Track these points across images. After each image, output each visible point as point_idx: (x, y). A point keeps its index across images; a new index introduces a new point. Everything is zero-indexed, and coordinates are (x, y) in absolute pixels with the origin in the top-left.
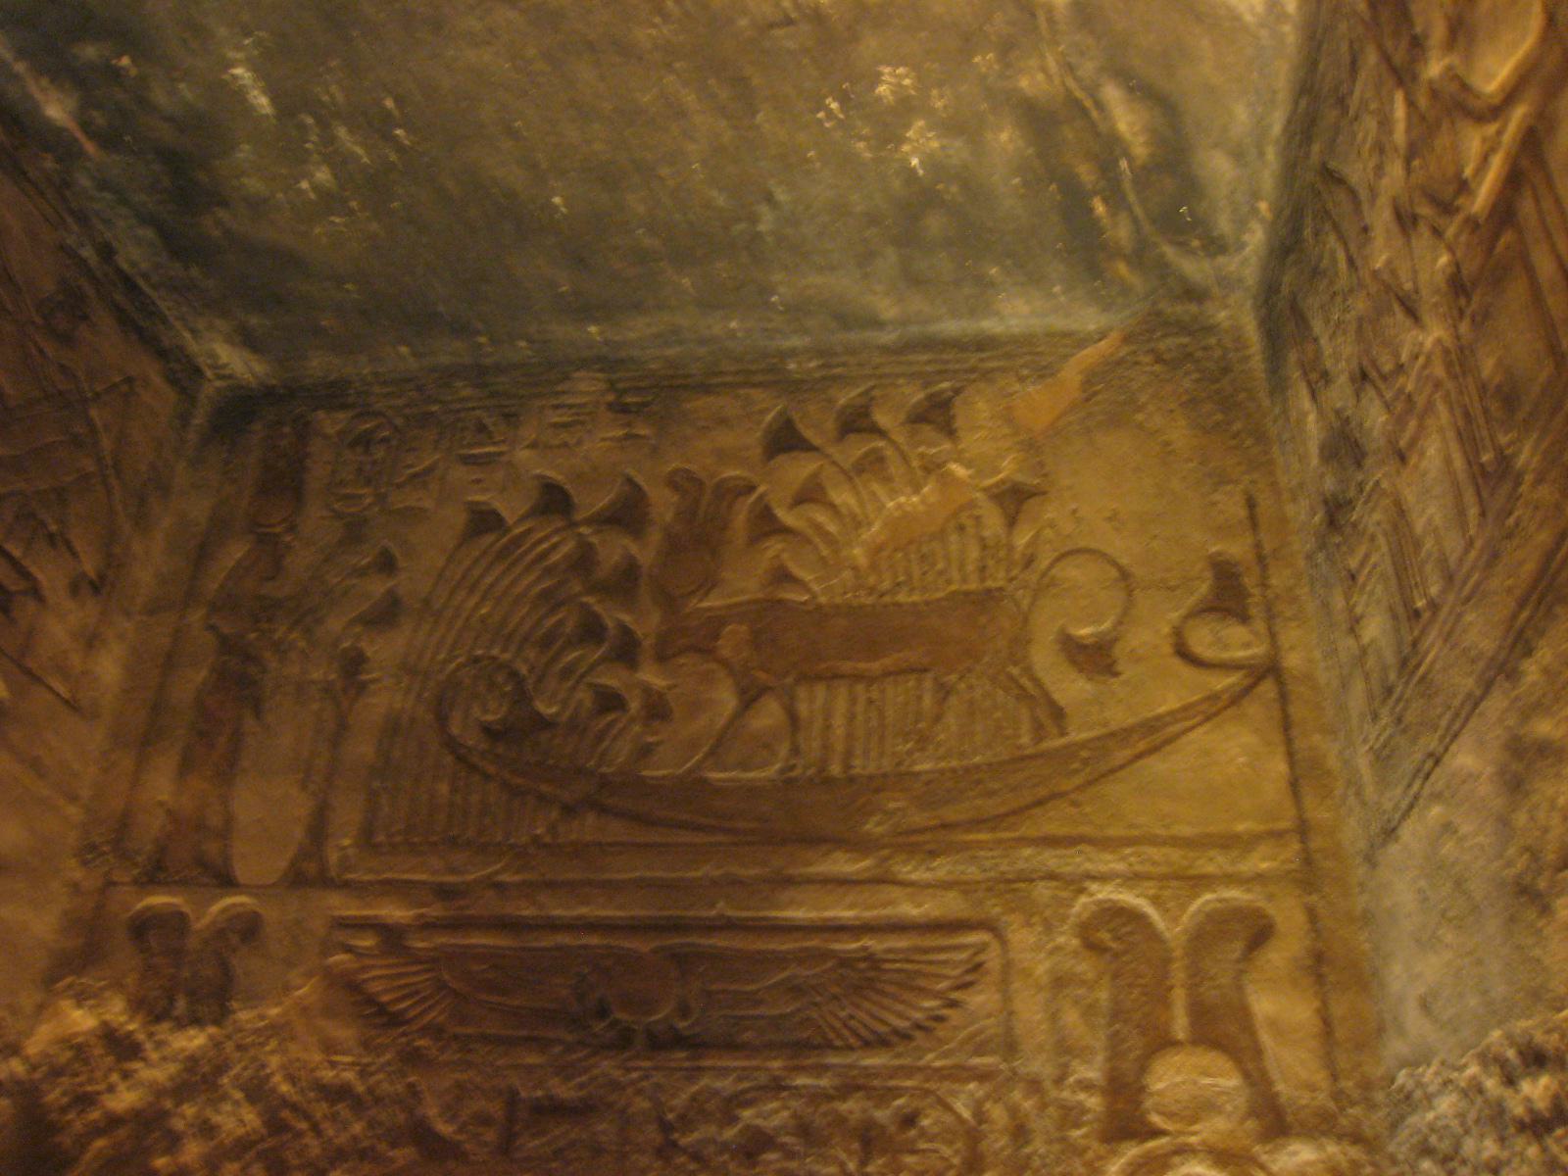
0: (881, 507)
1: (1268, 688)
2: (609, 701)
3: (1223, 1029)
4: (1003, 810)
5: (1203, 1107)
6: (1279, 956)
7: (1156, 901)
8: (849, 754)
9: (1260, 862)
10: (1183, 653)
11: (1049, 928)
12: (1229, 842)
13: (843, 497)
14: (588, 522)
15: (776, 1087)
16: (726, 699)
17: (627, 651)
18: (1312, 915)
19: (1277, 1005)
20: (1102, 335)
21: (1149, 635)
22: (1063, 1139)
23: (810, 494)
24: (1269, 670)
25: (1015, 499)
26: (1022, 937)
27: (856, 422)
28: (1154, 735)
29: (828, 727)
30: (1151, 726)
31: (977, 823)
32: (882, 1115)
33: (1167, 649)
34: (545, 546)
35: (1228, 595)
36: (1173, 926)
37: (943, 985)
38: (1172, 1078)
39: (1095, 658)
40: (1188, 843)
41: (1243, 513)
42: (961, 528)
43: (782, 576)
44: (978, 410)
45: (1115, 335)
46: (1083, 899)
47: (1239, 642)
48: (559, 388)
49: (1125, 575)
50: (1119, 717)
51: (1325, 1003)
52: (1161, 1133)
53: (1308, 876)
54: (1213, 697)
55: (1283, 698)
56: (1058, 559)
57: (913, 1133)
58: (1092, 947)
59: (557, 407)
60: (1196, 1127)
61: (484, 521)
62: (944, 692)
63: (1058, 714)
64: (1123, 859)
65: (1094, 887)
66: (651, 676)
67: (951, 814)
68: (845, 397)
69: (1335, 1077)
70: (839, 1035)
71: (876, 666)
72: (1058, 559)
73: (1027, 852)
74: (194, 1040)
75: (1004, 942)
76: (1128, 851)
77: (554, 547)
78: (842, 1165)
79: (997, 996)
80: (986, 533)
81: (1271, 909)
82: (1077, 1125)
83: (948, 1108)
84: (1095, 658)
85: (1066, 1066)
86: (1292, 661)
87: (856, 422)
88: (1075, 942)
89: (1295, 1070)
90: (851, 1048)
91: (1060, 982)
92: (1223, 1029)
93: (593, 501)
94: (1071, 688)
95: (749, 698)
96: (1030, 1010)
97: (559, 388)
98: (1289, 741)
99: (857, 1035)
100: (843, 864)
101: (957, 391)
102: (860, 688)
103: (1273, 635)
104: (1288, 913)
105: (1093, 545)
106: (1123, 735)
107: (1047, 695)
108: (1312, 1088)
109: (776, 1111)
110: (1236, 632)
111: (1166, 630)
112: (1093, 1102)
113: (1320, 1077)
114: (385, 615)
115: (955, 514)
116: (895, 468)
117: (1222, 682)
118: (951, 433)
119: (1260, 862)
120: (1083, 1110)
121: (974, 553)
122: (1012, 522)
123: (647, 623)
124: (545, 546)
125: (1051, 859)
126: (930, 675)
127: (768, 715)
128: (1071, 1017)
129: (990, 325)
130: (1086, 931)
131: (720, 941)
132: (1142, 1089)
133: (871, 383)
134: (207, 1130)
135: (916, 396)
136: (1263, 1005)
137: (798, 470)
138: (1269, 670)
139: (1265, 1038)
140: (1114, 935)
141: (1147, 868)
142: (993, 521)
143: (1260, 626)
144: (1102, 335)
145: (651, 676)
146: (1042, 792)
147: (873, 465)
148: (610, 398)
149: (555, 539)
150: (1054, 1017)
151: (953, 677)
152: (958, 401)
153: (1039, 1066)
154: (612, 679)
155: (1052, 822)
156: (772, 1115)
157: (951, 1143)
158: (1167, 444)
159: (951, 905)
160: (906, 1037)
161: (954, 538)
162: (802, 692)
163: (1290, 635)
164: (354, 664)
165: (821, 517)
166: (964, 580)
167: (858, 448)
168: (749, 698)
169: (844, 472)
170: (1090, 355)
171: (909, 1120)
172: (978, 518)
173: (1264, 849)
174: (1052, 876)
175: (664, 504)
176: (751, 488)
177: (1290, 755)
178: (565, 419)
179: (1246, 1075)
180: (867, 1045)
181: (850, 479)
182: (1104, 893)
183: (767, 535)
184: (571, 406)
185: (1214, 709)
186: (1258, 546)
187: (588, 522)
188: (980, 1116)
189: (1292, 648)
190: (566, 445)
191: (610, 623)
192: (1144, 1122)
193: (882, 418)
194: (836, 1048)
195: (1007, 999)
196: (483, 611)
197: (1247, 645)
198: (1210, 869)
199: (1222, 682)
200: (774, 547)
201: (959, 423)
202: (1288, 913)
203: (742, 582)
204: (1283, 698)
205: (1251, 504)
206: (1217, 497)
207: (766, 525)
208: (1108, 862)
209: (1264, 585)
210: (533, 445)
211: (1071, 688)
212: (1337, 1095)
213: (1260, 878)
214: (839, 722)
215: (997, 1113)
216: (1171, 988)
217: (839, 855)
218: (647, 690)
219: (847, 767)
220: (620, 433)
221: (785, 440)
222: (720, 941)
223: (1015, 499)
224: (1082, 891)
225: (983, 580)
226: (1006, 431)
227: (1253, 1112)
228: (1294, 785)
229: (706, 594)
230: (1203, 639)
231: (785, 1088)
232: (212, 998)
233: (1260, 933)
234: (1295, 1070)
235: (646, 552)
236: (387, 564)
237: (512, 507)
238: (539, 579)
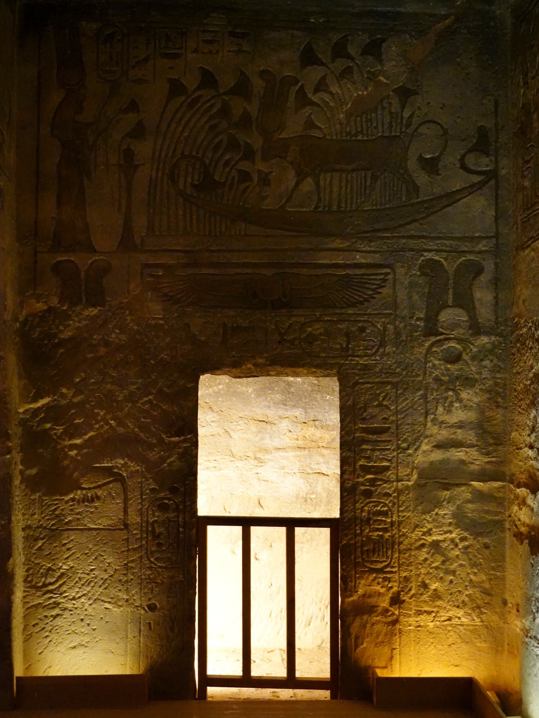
0: (351, 96)
1: (492, 182)
2: (245, 176)
3: (465, 302)
4: (396, 225)
5: (456, 325)
6: (484, 278)
7: (446, 259)
8: (340, 202)
9: (481, 247)
10: (464, 167)
11: (409, 268)
12: (472, 239)
13: (335, 89)
14: (225, 93)
15: (318, 321)
16: (291, 177)
17: (249, 154)
18: (496, 264)
19: (483, 296)
20: (446, 17)
21: (451, 159)
22: (412, 336)
23: (321, 86)
24: (492, 175)
25: (405, 94)
26: (400, 271)
27: (339, 51)
28: (451, 198)
29: (331, 191)
30: (449, 195)
31: (385, 230)
32: (354, 329)
33: (458, 165)
34: (208, 105)
35: (482, 144)
36: (450, 267)
37: (374, 287)
38: (446, 316)
39: (431, 166)
40: (459, 239)
41: (493, 109)
42: (384, 108)
43: (310, 124)
44: (392, 49)
45: (453, 17)
46: (422, 258)
47: (484, 163)
48: (205, 21)
49: (445, 131)
50: (438, 191)
51: (497, 294)
52: (442, 334)
53: (496, 252)
54: (472, 186)
55: (497, 187)
56: (421, 124)
57: (364, 334)
58: (423, 274)
59: (204, 31)
60: (453, 333)
61: (176, 88)
62: (375, 178)
63: (417, 189)
64: (437, 244)
65: (426, 254)
66: (261, 166)
67: (377, 226)
68: (335, 37)
69: (497, 319)
70: (340, 304)
71: (350, 167)
72: (421, 124)
73: (404, 241)
74: (94, 311)
75: (395, 273)
76: (438, 242)
77: (213, 105)
78: (341, 344)
79: (392, 291)
80: (393, 110)
81: (484, 263)
82: (417, 332)
83: (376, 326)
84: (431, 166)
85: (414, 313)
86: (503, 172)
87: (339, 51)
88: (419, 273)
89: (485, 314)
90: (343, 308)
91: (412, 285)
92: (465, 302)
93: (227, 81)
94: (422, 178)
95: (301, 177)
96: (402, 294)
97: (205, 21)
98: (497, 205)
99: (345, 303)
100: (338, 243)
101: (384, 40)
102: (344, 175)
103: (497, 161)
104: (489, 265)
105: (436, 119)
106: (440, 197)
107: (413, 182)
108: (489, 320)
109: (318, 329)
110: (485, 160)
111: (459, 158)
112: (421, 324)
113: (493, 318)
114: (138, 132)
115: (381, 101)
116: (356, 76)
117: (476, 179)
118: (380, 60)
119: (481, 247)
120: (418, 326)
121: (387, 119)
122: (403, 108)
123: (257, 142)
124: (208, 105)
125: (412, 243)
126: (371, 171)
127: (308, 184)
128: (416, 297)
129: (402, 10)
130: (421, 267)
131: (295, 271)
132: (438, 321)
133: (348, 33)
134: (107, 344)
135: (364, 39)
136: (478, 295)
137: (315, 74)
138: (492, 175)
139: (477, 305)
140: (432, 269)
141: (443, 248)
142: (395, 102)
143: (493, 159)
144: (446, 17)
145: (261, 166)
146: (409, 219)
147: (346, 73)
148: (230, 29)
149: (213, 101)
150: (410, 298)
151: (379, 173)
152: (384, 45)
153: (405, 312)
154: (245, 166)
155: (412, 229)
156: (317, 329)
157: (377, 338)
158: (468, 74)
159: (376, 258)
160: (362, 303)
161: (380, 112)
162: (322, 177)
163: (504, 162)
164: (129, 155)
165: (327, 97)
166: (383, 132)
167: (340, 64)
168: (301, 177)
169: (336, 76)
170: (440, 26)
171: (362, 330)
172: (391, 103)
173: (484, 242)
174: (412, 250)
175: (258, 85)
176: (299, 81)
177: (496, 211)
178: (209, 38)
179: (470, 317)
180: (349, 306)
181: (337, 79)
182: (428, 255)
183: (304, 106)
184: (210, 31)
185: (472, 189)
186: (496, 124)
187: (225, 93)
188: (385, 328)
189: (503, 168)
190: (211, 52)
191: (242, 143)
192: (437, 330)
193: (352, 50)
194: (337, 308)
195: (394, 292)
196: (186, 134)
197: (487, 166)
198: (466, 249)
199: (476, 179)
200: (308, 110)
201: (384, 57)
202: (489, 265)
203: (293, 126)
204: (497, 187)
205: (496, 105)
206: (484, 101)
207: (303, 100)
208: (432, 245)
209: (496, 141)
210: (196, 51)
211: (422, 178)
212: (496, 323)
213: (480, 252)
214: (335, 189)
215: (390, 327)
216: (449, 289)
217: (338, 241)
218: (260, 171)
219: (339, 206)
220: (235, 48)
221: (309, 58)
222: (295, 271)
223: (405, 94)
224: (422, 255)
225: (391, 132)
226: (403, 62)
227: (470, 328)
228: (496, 219)
229: (281, 132)
230: (471, 161)
231: (321, 321)
232: (96, 297)
233: (479, 271)
234: (485, 314)
235: (253, 109)
236: (133, 106)
237: (191, 82)
238: (208, 121)
